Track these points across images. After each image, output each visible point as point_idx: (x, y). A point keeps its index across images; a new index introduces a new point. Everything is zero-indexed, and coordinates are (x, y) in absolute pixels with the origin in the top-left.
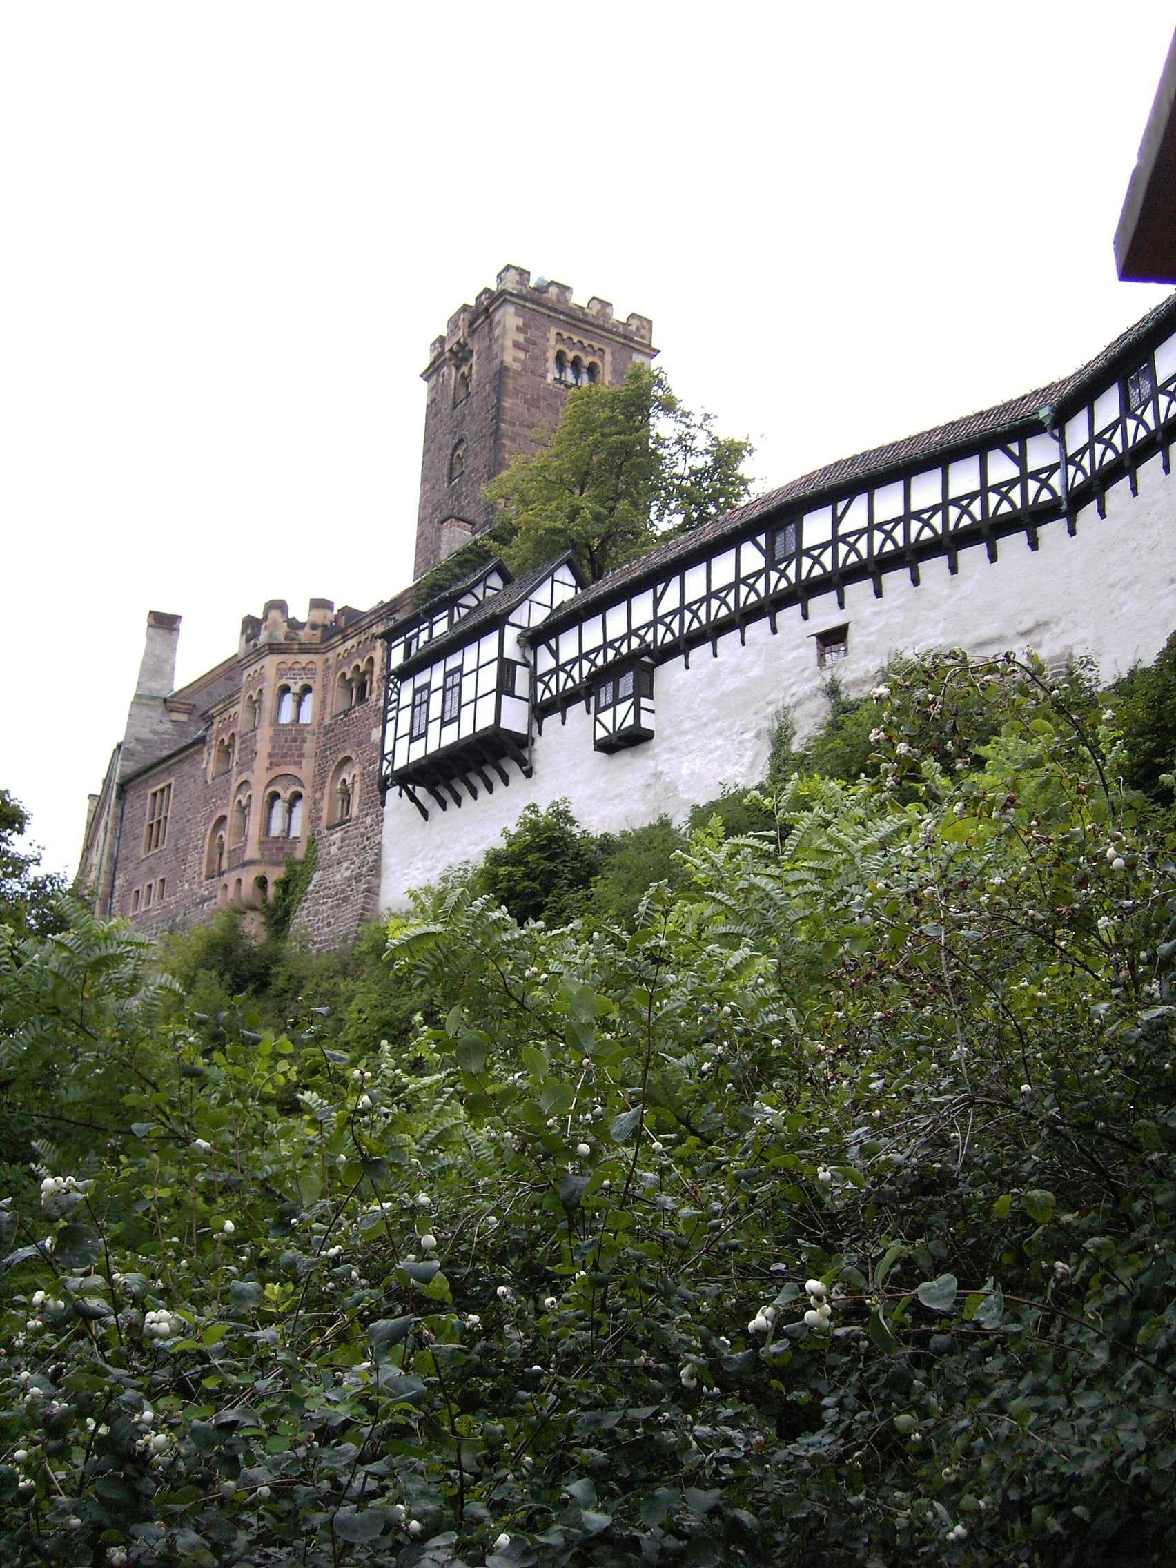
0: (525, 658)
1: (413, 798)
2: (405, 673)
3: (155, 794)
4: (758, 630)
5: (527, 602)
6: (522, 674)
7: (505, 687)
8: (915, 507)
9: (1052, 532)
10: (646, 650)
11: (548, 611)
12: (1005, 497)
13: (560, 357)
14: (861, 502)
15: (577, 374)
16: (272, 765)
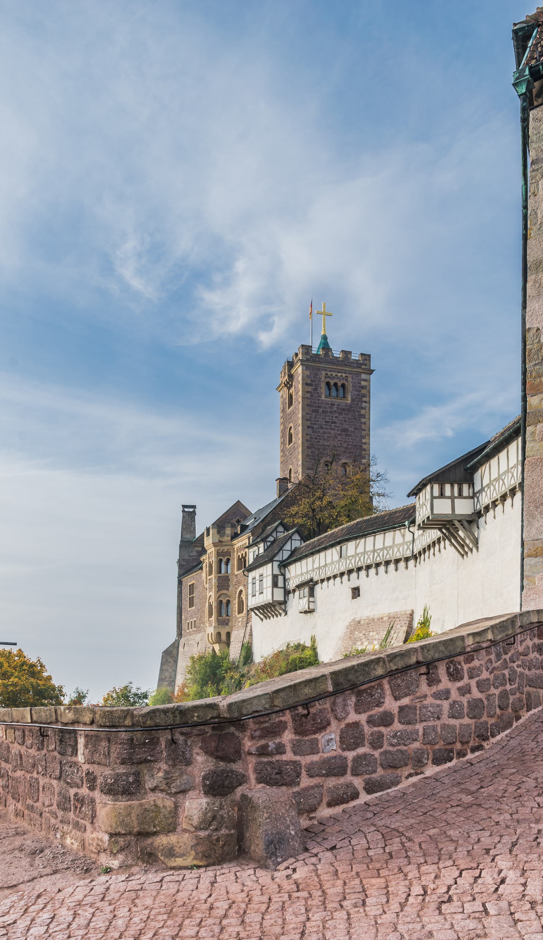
0: (281, 572)
1: (256, 614)
2: (251, 569)
3: (190, 585)
4: (338, 579)
5: (281, 551)
6: (281, 578)
7: (275, 584)
8: (376, 548)
9: (411, 563)
10: (311, 580)
11: (290, 552)
12: (399, 550)
13: (328, 384)
14: (363, 540)
15: (337, 390)
16: (219, 590)
